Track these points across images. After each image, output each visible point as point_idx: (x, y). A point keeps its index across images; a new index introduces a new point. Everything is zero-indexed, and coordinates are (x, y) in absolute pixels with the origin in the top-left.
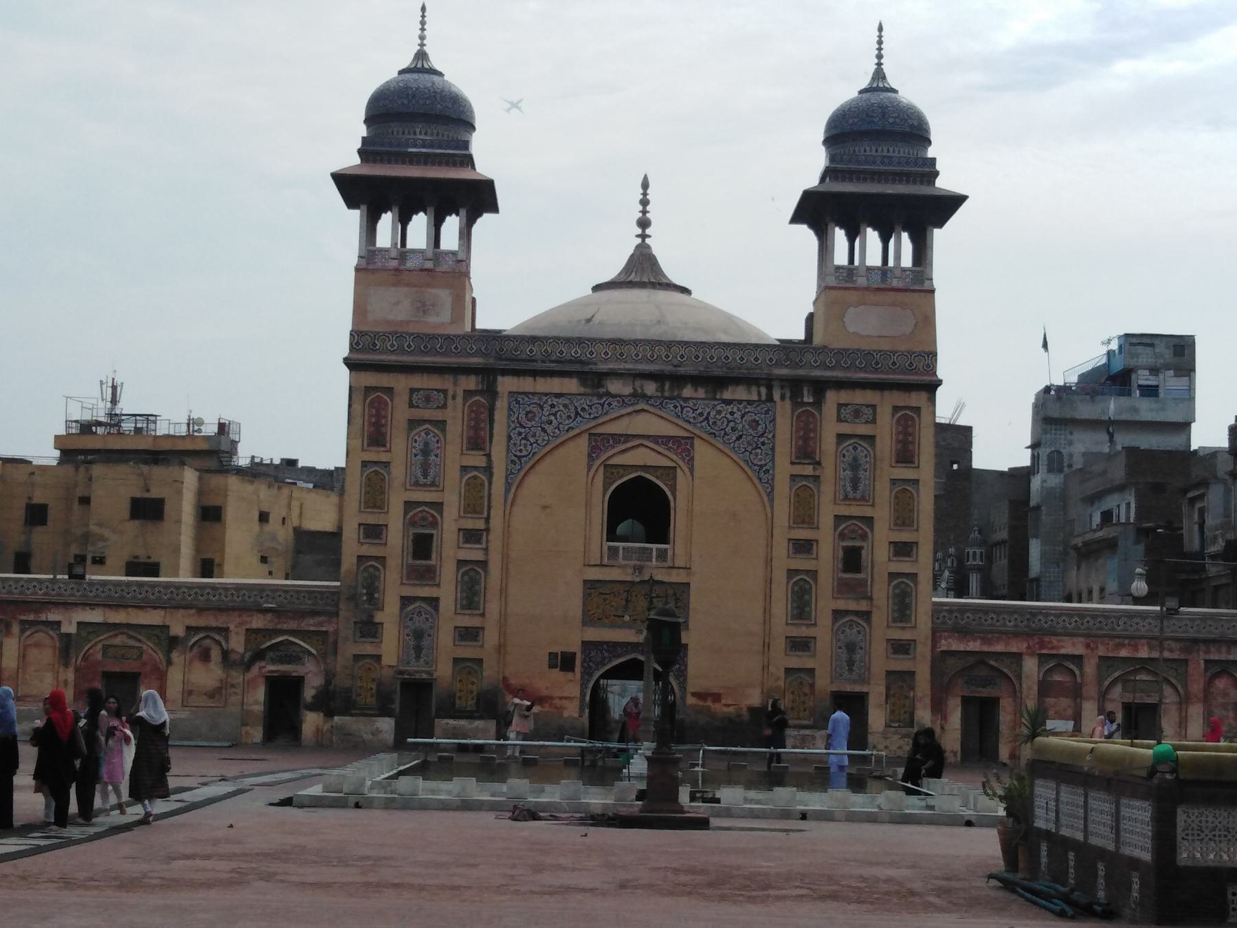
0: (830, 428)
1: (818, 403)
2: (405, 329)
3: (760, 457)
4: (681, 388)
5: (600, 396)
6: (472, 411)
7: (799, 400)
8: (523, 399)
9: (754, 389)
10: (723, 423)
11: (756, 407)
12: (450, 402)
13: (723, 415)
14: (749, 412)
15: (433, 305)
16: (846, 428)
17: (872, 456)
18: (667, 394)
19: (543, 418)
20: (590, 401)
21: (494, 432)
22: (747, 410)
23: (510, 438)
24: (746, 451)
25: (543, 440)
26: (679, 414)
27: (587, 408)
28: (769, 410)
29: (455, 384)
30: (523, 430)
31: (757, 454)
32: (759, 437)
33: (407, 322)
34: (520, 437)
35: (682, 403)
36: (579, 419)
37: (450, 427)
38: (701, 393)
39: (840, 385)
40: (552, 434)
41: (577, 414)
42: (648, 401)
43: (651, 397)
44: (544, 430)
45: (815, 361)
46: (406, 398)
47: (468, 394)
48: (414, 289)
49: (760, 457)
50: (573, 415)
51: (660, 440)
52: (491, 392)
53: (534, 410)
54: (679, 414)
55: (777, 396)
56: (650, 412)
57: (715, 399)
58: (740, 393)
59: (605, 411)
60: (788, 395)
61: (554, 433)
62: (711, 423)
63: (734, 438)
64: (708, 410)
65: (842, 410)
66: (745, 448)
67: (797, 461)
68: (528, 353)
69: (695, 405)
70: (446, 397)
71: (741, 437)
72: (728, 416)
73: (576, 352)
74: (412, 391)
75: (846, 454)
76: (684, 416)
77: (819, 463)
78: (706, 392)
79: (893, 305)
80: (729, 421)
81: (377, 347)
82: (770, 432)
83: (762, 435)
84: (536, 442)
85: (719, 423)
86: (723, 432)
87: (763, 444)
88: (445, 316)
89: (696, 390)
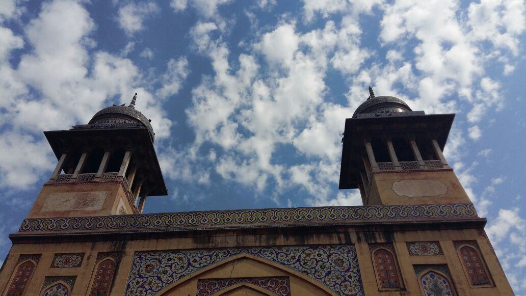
0: (406, 260)
1: (390, 242)
2: (65, 216)
3: (349, 288)
4: (275, 239)
5: (209, 249)
6: (102, 268)
7: (373, 242)
8: (146, 256)
9: (335, 236)
10: (312, 263)
11: (339, 249)
12: (85, 261)
13: (312, 256)
14: (333, 253)
15: (92, 201)
16: (420, 260)
17: (450, 280)
18: (263, 244)
19: (160, 269)
20: (201, 254)
21: (116, 282)
22: (331, 252)
23: (128, 286)
24: (336, 284)
25: (157, 287)
26: (275, 258)
27: (198, 259)
28: (349, 251)
29: (92, 249)
30: (142, 279)
31: (346, 286)
32: (346, 272)
33: (69, 212)
34: (138, 286)
35: (276, 250)
36: (191, 268)
37: (78, 280)
38: (292, 241)
39: (404, 228)
40: (166, 282)
41: (189, 264)
42: (248, 251)
43: (251, 247)
44: (159, 279)
45: (379, 214)
46: (50, 261)
47: (101, 255)
48: (82, 193)
49: (349, 288)
50: (185, 266)
51: (260, 282)
52: (119, 254)
53: (153, 264)
54: (275, 258)
55: (354, 238)
56: (250, 259)
57: (304, 245)
58: (324, 240)
59: (213, 260)
60: (363, 239)
61: (168, 280)
62: (302, 264)
63: (324, 274)
64: (299, 254)
65: (412, 247)
66: (335, 282)
67: (383, 289)
68: (156, 224)
69: (287, 251)
70: (82, 259)
71: (329, 272)
72: (316, 257)
73: (193, 221)
74: (57, 255)
75: (426, 282)
76: (279, 260)
77: (404, 289)
78: (295, 241)
79: (426, 178)
80: (317, 262)
81: (40, 228)
82: (354, 267)
83: (348, 270)
84: (151, 289)
85: (309, 263)
86: (314, 270)
87: (350, 277)
88: (98, 206)
89: (287, 240)
